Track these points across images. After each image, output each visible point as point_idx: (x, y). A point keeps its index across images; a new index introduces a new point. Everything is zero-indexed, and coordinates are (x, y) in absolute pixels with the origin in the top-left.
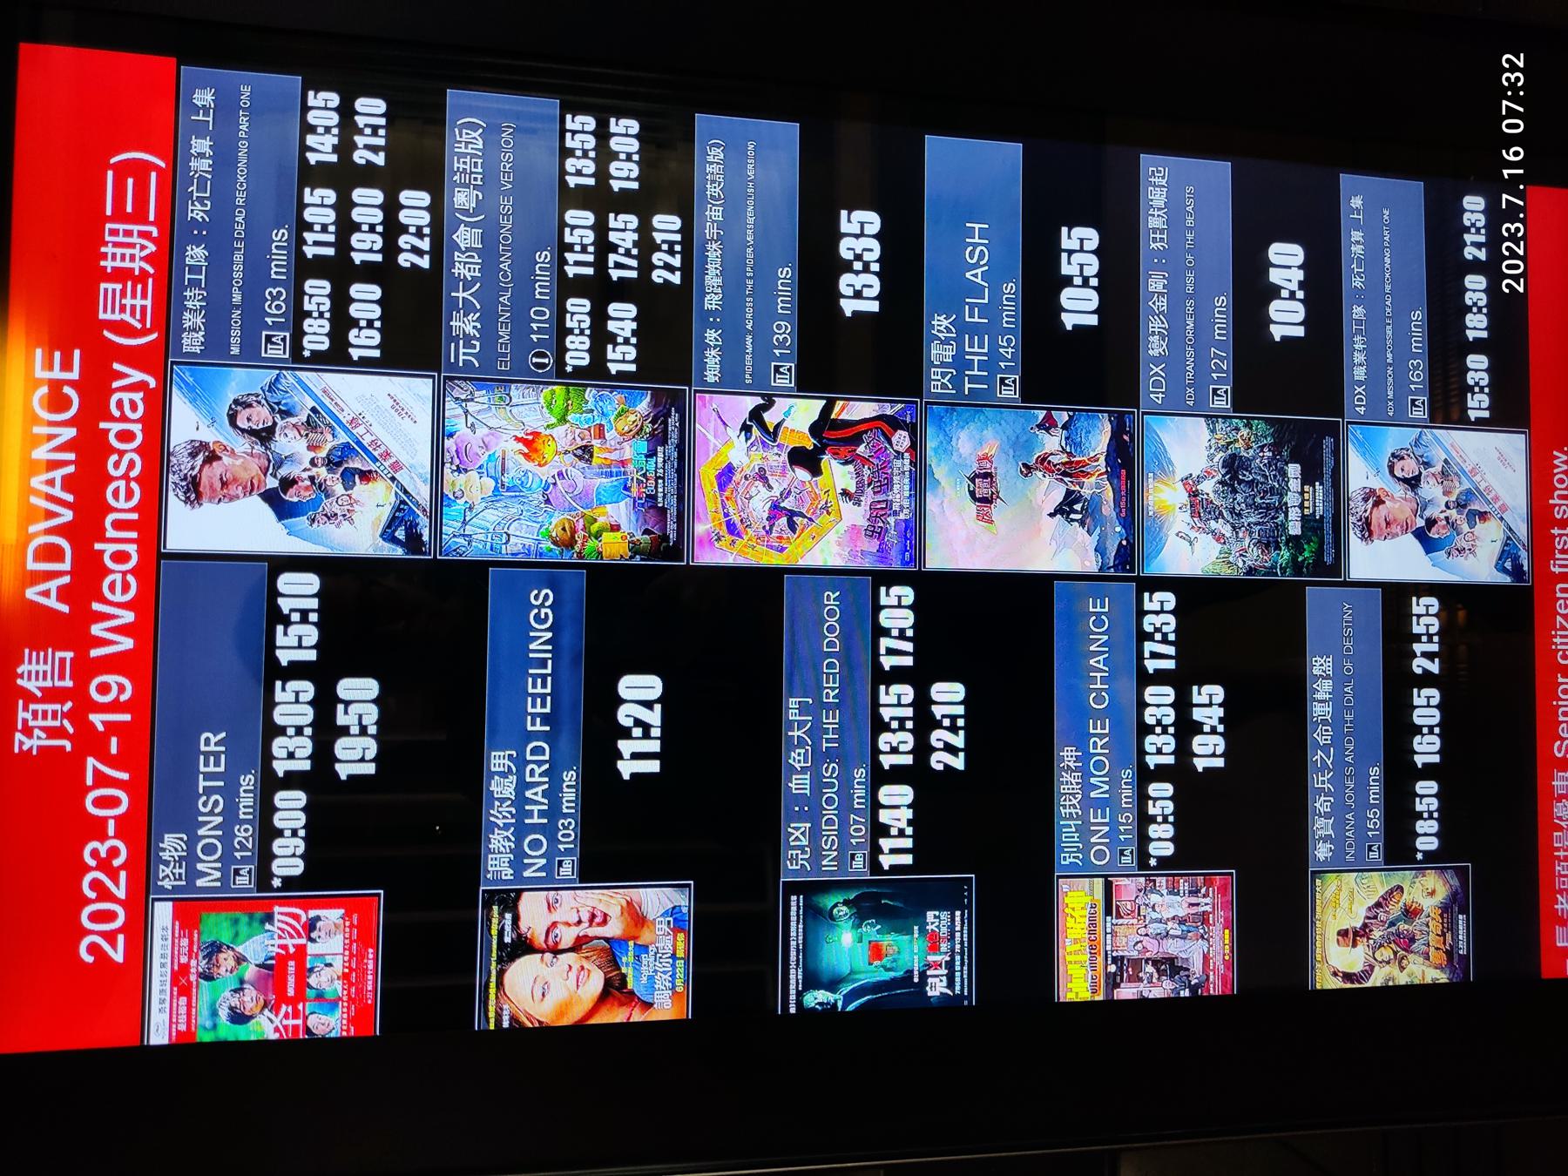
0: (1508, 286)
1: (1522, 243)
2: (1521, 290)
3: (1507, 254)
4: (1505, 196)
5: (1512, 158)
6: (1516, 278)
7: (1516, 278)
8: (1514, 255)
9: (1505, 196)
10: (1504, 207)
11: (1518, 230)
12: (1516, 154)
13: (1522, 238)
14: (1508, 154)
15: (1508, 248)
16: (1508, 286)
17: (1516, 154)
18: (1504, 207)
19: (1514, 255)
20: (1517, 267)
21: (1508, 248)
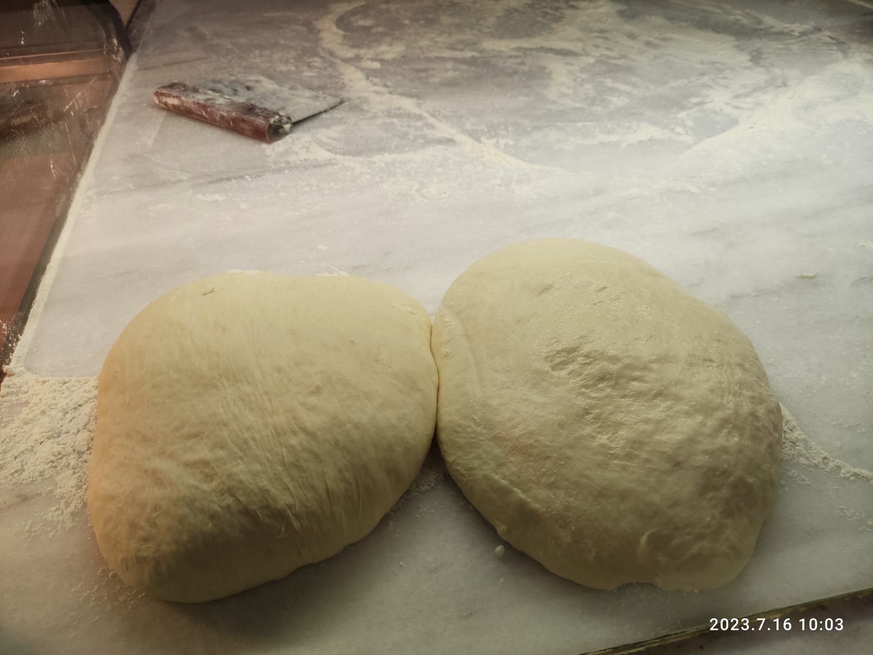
0: (714, 622)
1: (738, 629)
2: (712, 629)
3: (732, 621)
4: (764, 620)
5: (785, 624)
6: (718, 626)
7: (718, 626)
8: (731, 625)
9: (764, 620)
10: (758, 619)
11: (745, 627)
12: (787, 626)
13: (740, 629)
14: (787, 622)
15: (735, 622)
16: (714, 622)
17: (787, 626)
18: (758, 619)
19: (731, 625)
20: (724, 626)
21: (735, 622)
